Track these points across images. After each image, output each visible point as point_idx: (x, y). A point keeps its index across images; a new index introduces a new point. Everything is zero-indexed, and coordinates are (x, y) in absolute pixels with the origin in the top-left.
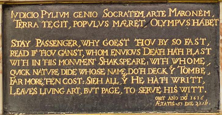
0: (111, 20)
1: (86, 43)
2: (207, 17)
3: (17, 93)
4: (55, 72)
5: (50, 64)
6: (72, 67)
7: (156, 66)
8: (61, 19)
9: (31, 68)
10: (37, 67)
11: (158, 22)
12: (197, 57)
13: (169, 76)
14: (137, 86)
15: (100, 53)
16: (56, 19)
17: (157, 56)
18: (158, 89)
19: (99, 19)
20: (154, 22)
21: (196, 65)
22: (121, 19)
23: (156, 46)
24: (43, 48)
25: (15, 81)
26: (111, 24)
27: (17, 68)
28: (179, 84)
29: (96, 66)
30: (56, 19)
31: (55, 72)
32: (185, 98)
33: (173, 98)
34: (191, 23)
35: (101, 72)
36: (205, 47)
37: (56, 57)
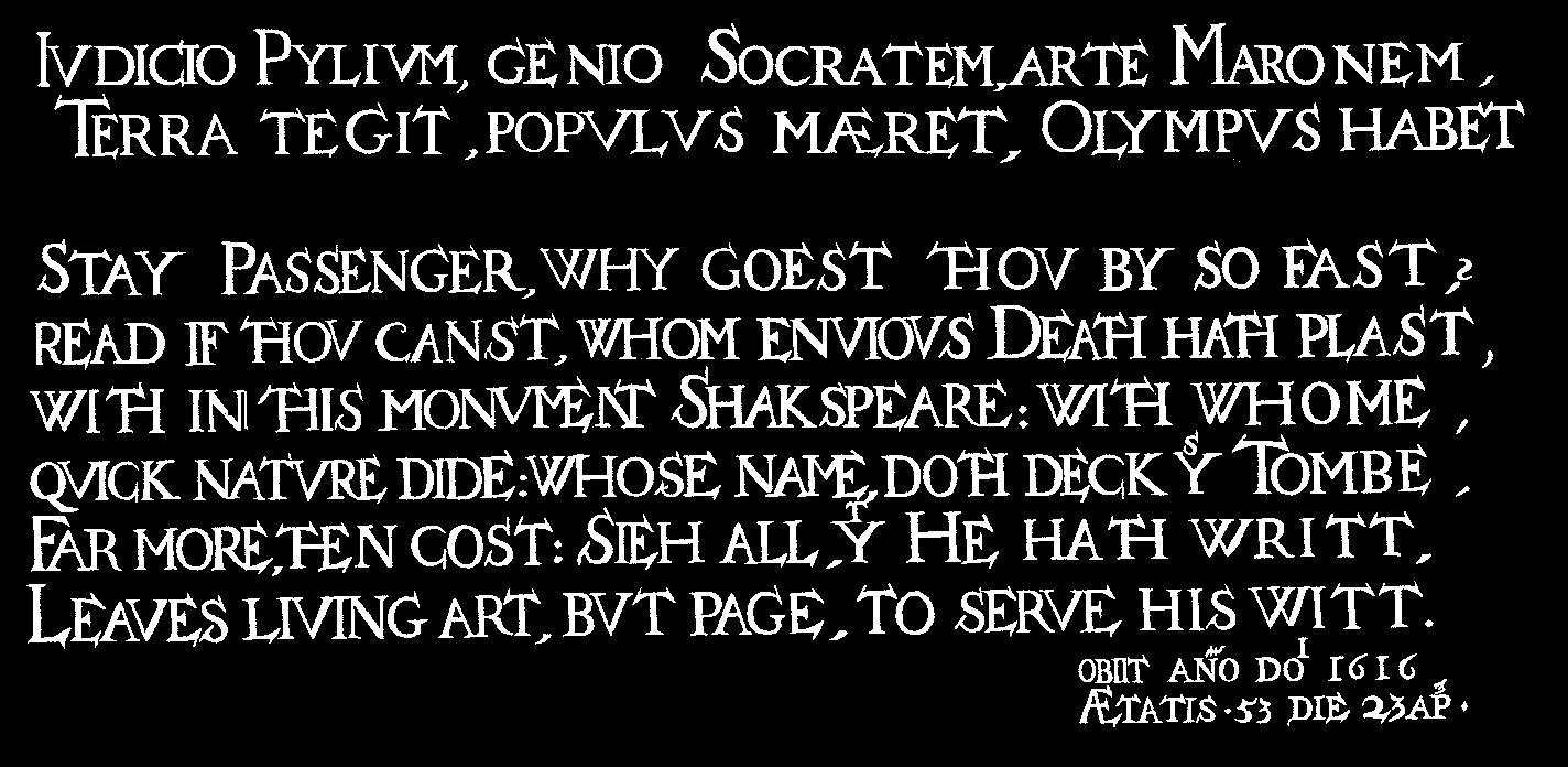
0: (759, 105)
1: (575, 268)
2: (1444, 92)
4: (350, 479)
5: (321, 410)
6: (476, 442)
7: (1083, 437)
9: (180, 447)
11: (1093, 123)
12: (1371, 371)
13: (1177, 508)
14: (946, 581)
15: (682, 339)
16: (363, 96)
17: (1086, 371)
18: (1087, 602)
20: (1067, 126)
21: (1371, 434)
22: (830, 102)
23: (1083, 296)
24: (269, 305)
26: (759, 131)
28: (1242, 571)
30: (363, 96)
31: (350, 479)
34: (1330, 128)
35: (687, 478)
36: (1433, 296)
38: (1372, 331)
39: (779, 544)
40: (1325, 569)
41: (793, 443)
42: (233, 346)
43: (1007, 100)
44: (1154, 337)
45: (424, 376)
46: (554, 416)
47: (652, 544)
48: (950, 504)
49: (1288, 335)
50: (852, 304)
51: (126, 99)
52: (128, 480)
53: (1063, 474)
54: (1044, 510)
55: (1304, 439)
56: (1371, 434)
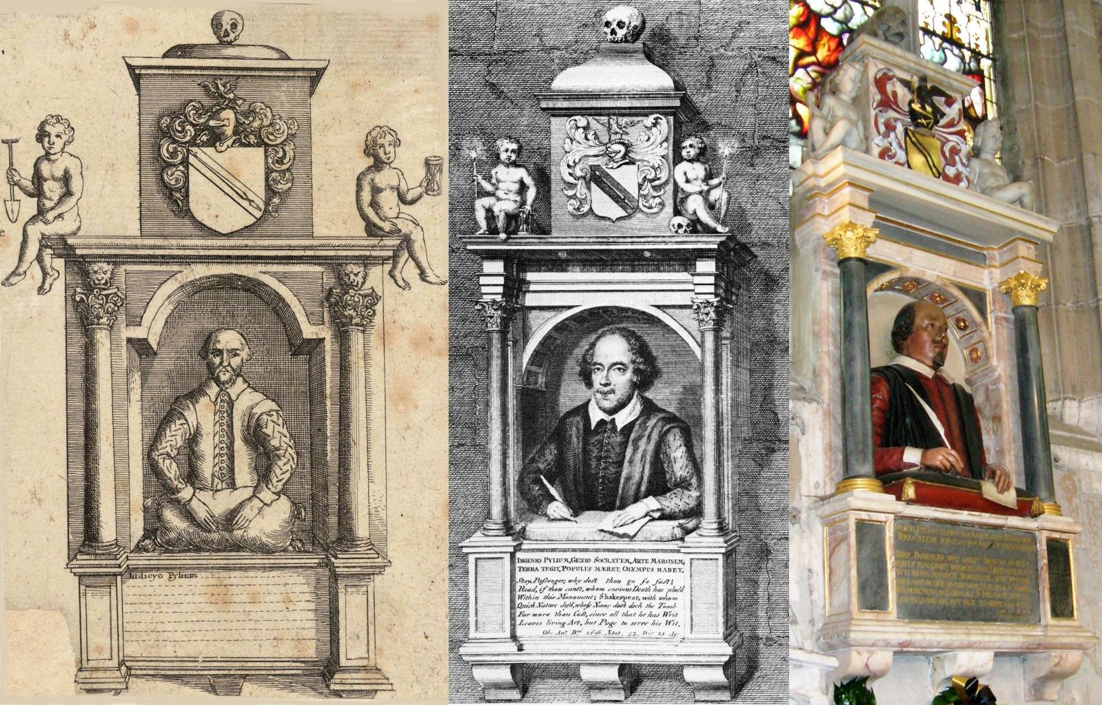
1: (950, 558)
14: (987, 600)
23: (997, 565)
24: (919, 560)
35: (962, 585)
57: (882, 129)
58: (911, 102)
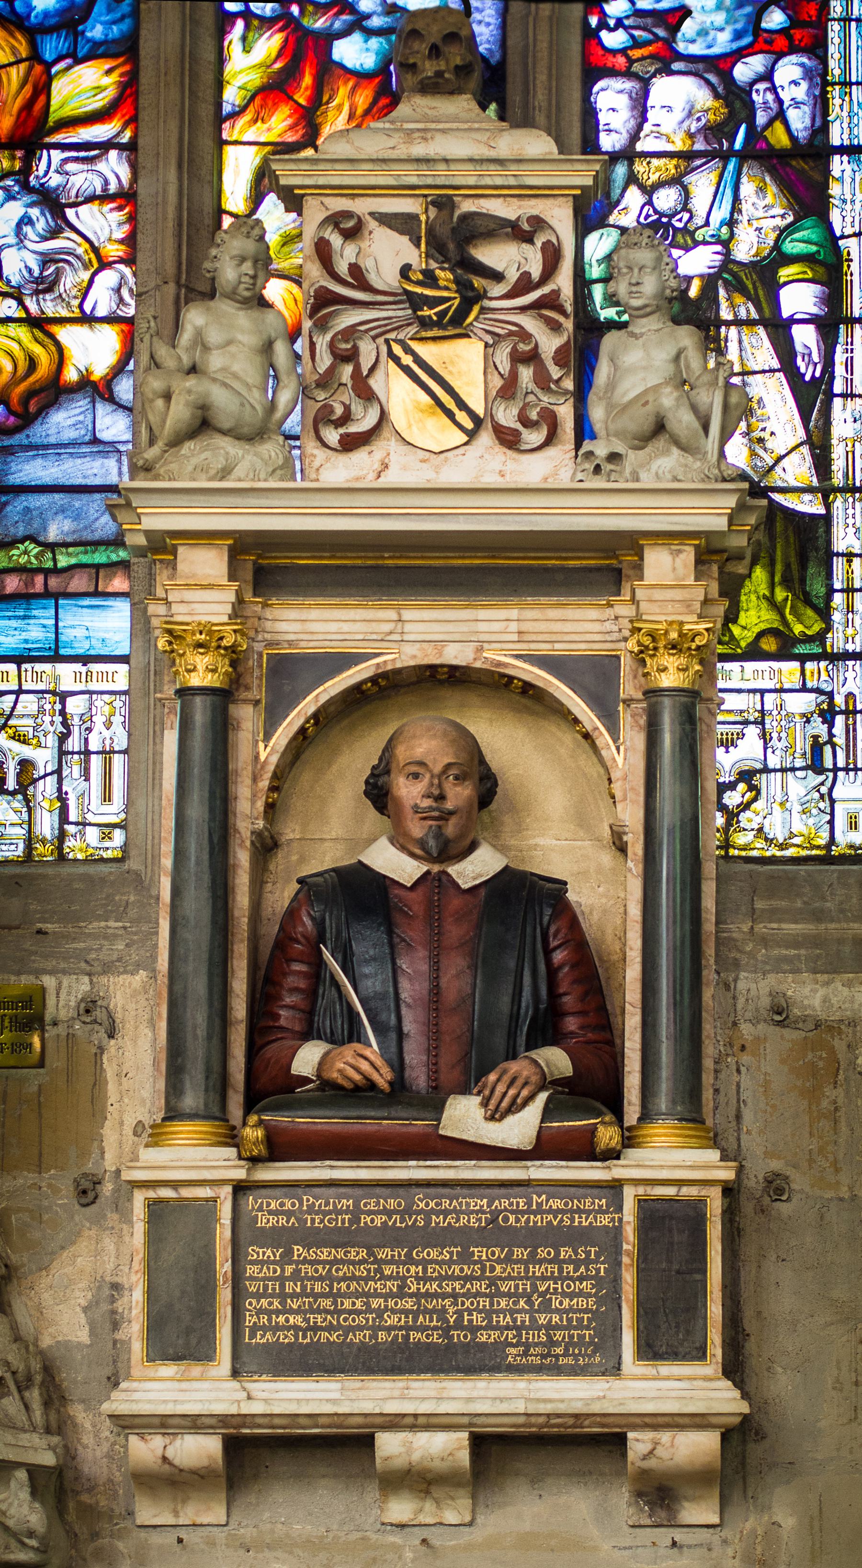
0: (428, 1214)
1: (383, 1254)
2: (600, 1211)
3: (258, 1339)
4: (326, 1303)
5: (318, 1288)
6: (357, 1295)
7: (509, 1295)
8: (339, 1212)
9: (283, 1296)
10: (294, 1295)
11: (512, 1218)
12: (581, 1279)
13: (531, 1312)
14: (474, 1329)
15: (408, 1271)
16: (330, 1212)
17: (510, 1278)
18: (511, 1334)
19: (408, 1211)
20: (506, 1219)
21: (580, 1294)
22: (446, 1213)
23: (508, 1260)
24: (305, 1261)
25: (255, 1319)
26: (428, 1221)
27: (258, 1296)
28: (549, 1327)
29: (401, 1294)
30: (330, 1212)
31: (326, 1303)
32: (559, 1351)
33: (539, 1350)
34: (572, 1220)
35: (409, 1304)
36: (596, 1261)
37: (329, 1278)
38: (582, 1269)
39: (431, 1320)
40: (569, 1327)
41: (436, 1295)
42: (297, 1271)
43: (491, 1212)
44: (527, 1270)
45: (344, 1279)
46: (376, 1289)
47: (400, 1320)
48: (474, 1310)
49: (561, 1270)
50: (450, 1262)
51: (270, 1212)
52: (270, 1304)
53: (503, 1304)
54: (497, 1312)
55: (564, 1294)
56: (580, 1294)
57: (325, 361)
58: (405, 271)
